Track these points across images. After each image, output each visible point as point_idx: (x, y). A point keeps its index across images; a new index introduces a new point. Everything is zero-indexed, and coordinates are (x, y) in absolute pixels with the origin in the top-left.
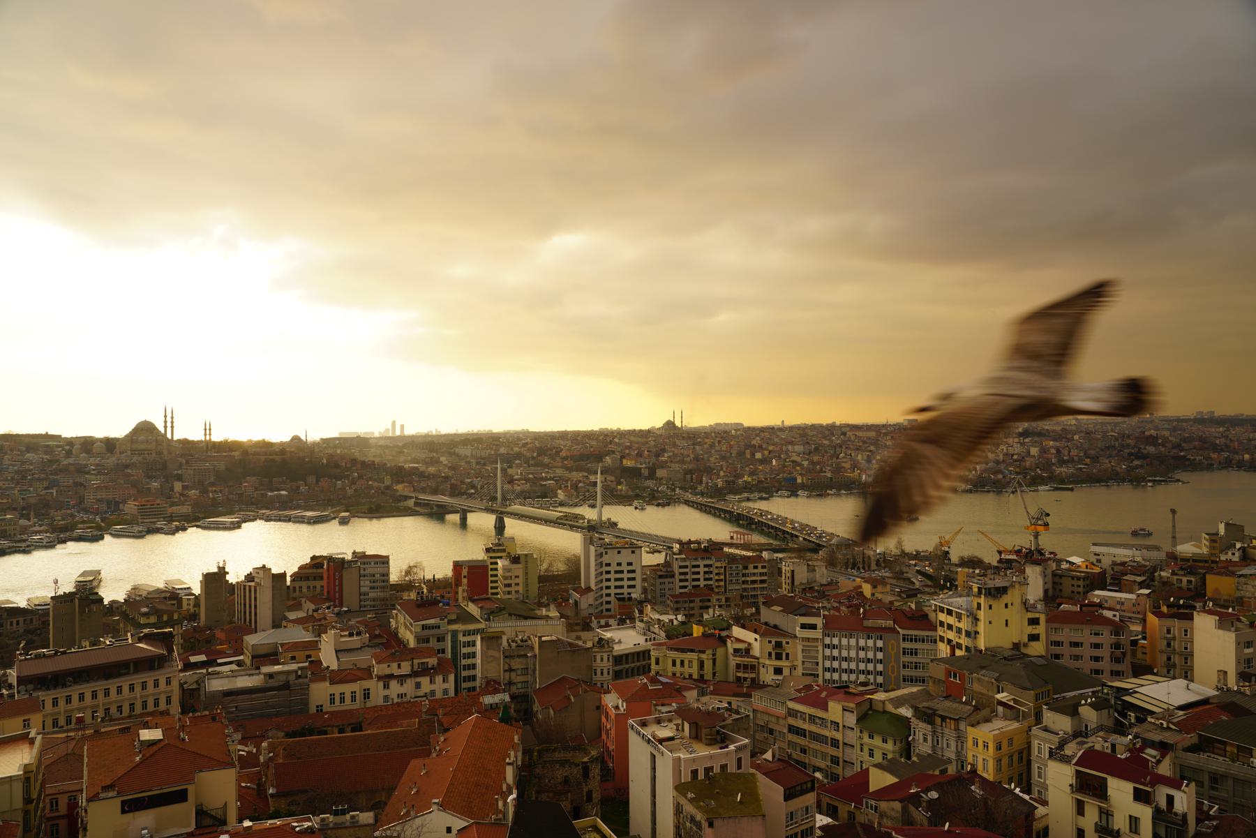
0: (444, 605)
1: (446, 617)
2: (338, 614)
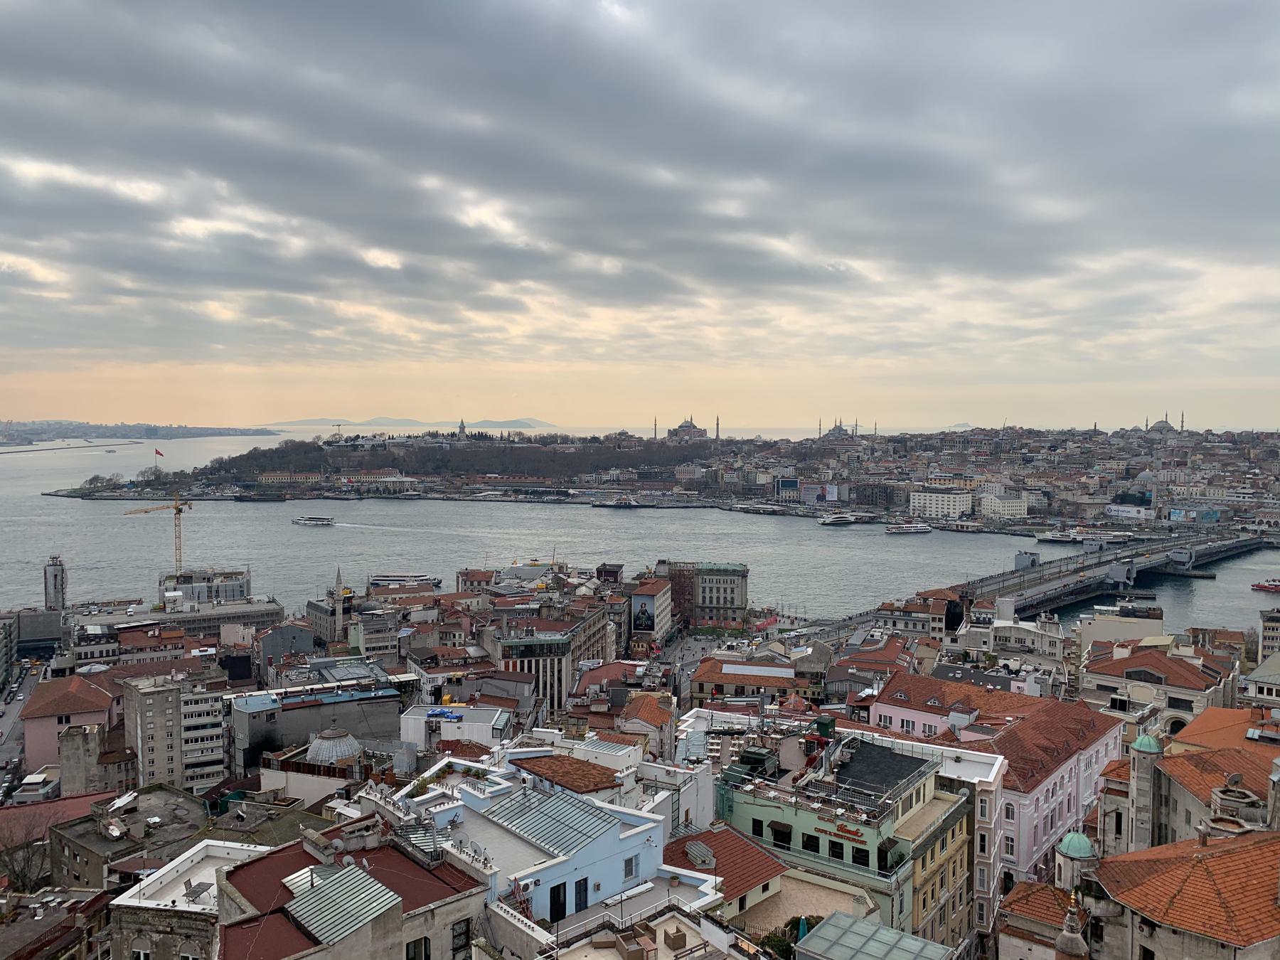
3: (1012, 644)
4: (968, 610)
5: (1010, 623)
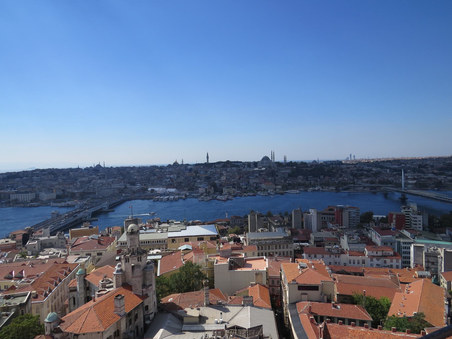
0: (393, 230)
1: (395, 235)
2: (341, 229)
3: (48, 245)
4: (32, 236)
5: (47, 238)
